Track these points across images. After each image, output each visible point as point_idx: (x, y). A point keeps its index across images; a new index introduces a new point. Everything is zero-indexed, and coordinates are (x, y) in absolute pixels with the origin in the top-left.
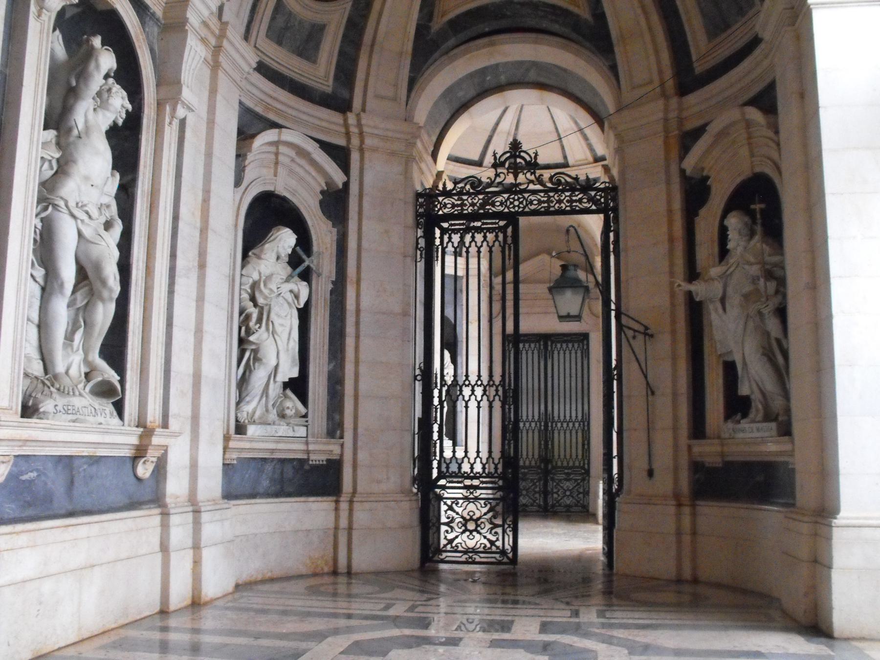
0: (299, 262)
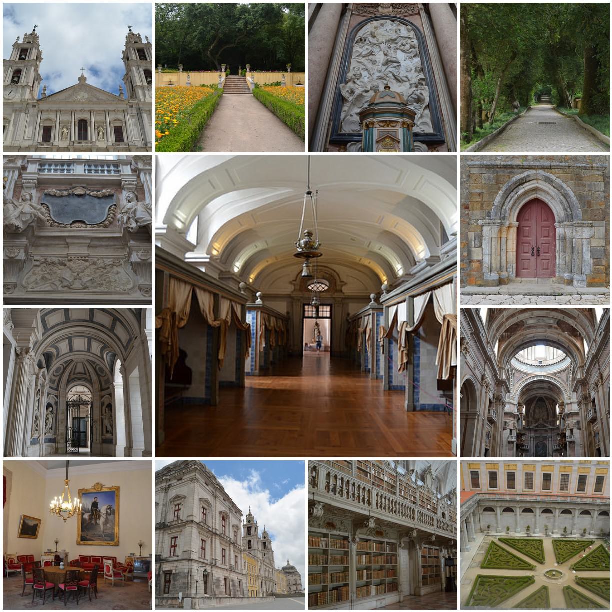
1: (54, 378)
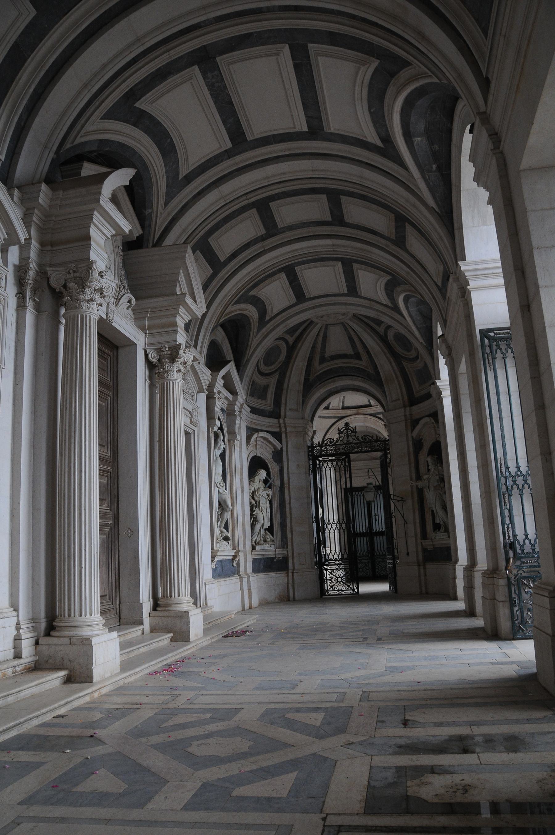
1: (261, 381)
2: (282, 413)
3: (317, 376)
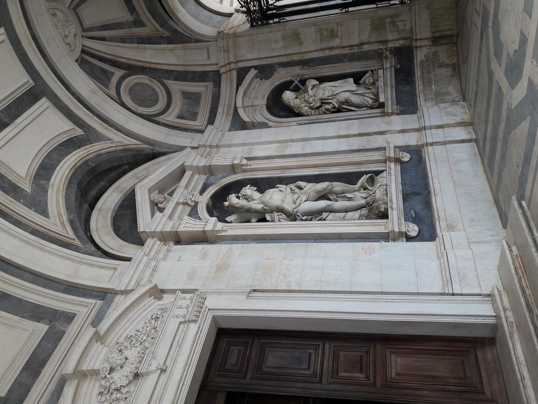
0: (298, 87)
2: (214, 68)
3: (160, 26)
